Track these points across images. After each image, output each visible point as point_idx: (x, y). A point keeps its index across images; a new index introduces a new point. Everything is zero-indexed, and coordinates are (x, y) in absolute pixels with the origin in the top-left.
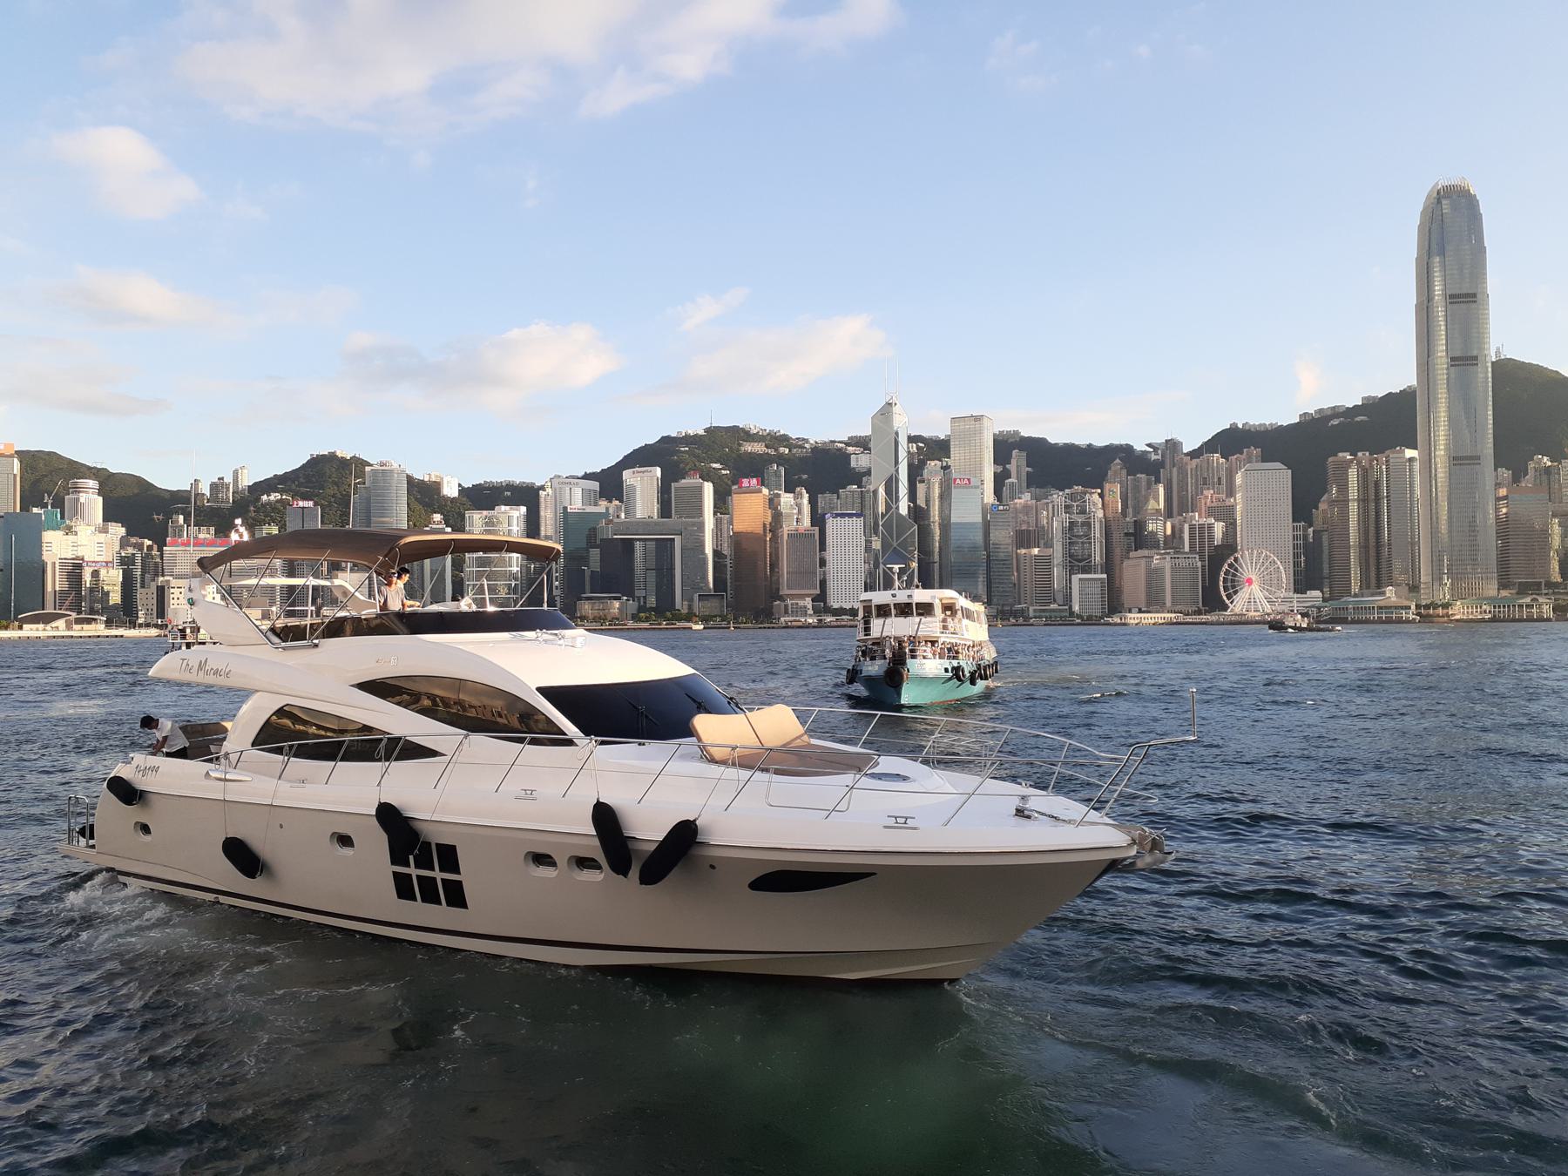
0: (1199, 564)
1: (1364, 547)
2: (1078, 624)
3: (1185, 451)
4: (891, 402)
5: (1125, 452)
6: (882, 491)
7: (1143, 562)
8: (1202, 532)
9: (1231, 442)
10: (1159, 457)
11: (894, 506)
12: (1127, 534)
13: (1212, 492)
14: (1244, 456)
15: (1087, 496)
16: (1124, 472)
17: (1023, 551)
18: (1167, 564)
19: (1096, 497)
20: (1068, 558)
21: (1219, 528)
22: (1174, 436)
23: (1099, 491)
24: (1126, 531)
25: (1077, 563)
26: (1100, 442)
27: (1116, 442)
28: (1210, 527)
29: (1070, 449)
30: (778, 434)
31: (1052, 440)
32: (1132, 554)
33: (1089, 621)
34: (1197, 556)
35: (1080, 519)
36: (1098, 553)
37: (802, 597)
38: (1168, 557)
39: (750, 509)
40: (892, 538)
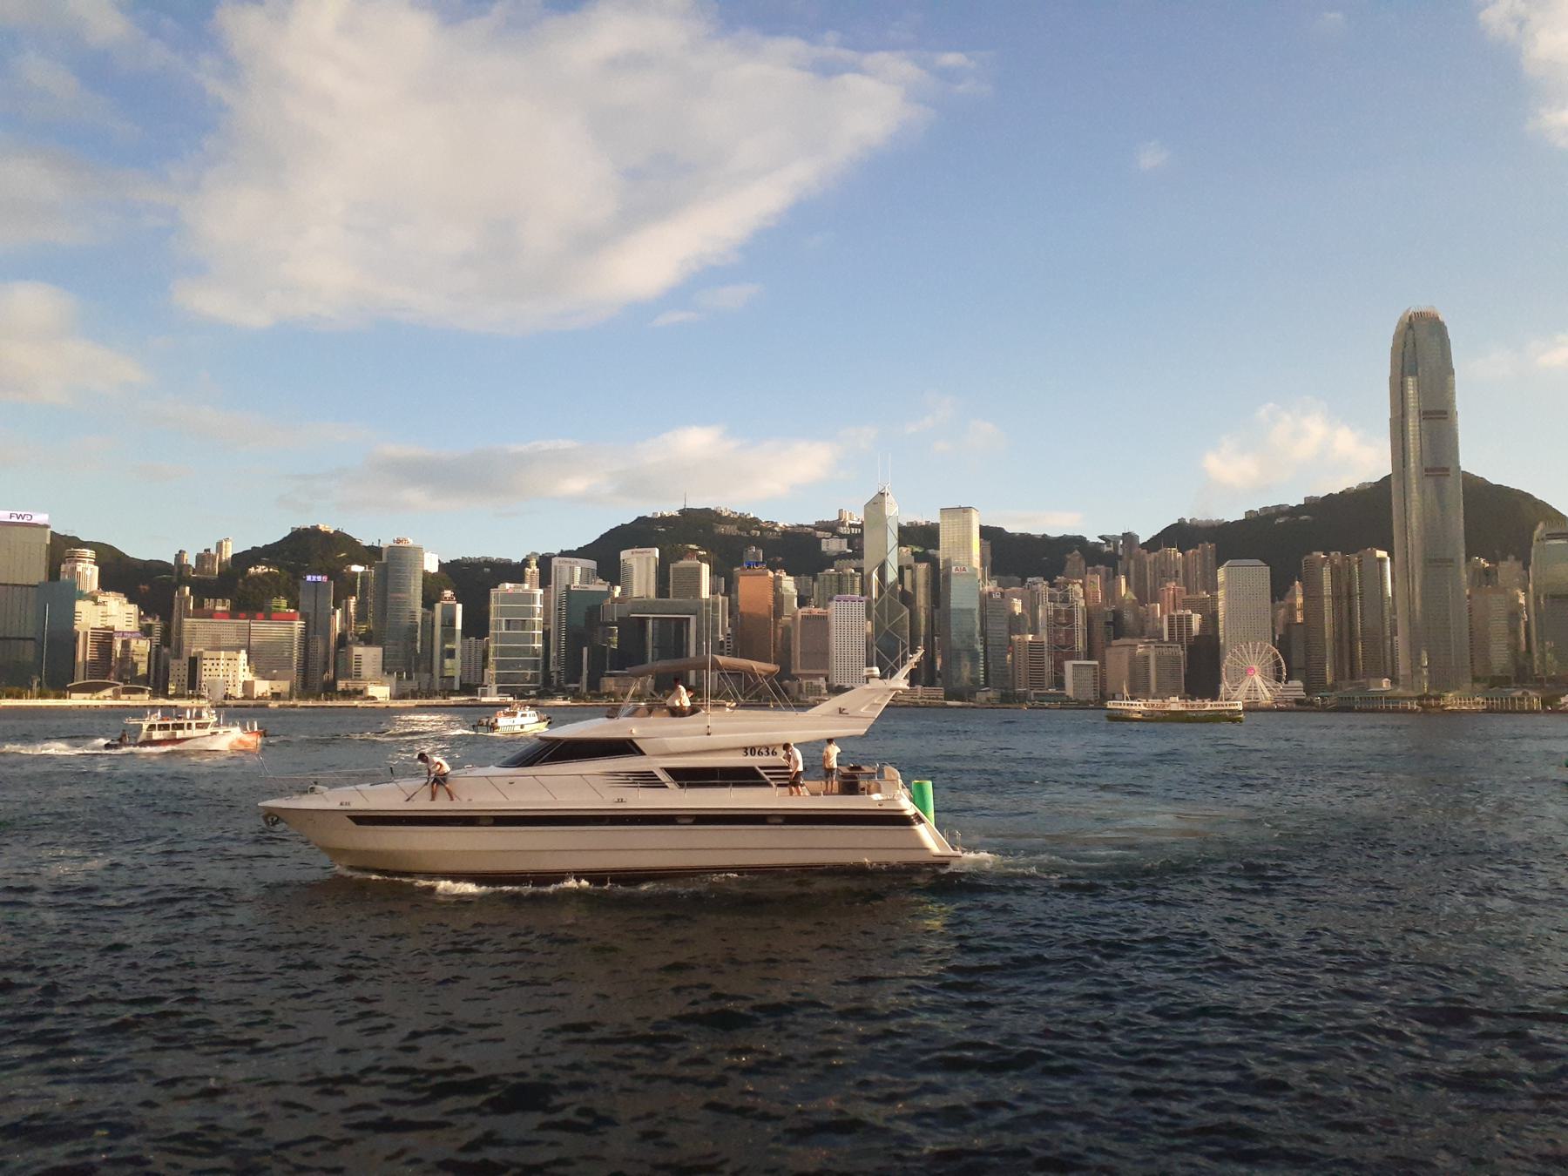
1: (1338, 639)
2: (1092, 709)
3: (1141, 542)
5: (1079, 541)
6: (875, 576)
7: (1127, 649)
8: (1177, 625)
9: (1180, 535)
10: (1111, 549)
12: (1108, 623)
13: (1174, 584)
14: (1198, 551)
15: (1070, 587)
16: (1083, 564)
17: (1017, 637)
19: (1077, 587)
21: (1196, 620)
22: (1131, 530)
23: (1081, 581)
26: (1054, 533)
27: (1069, 533)
28: (1189, 618)
29: (1026, 539)
30: (748, 517)
31: (1010, 529)
32: (1114, 642)
33: (1082, 705)
34: (1180, 646)
35: (1063, 607)
36: (1080, 640)
37: (817, 676)
38: (1152, 646)
39: (755, 587)
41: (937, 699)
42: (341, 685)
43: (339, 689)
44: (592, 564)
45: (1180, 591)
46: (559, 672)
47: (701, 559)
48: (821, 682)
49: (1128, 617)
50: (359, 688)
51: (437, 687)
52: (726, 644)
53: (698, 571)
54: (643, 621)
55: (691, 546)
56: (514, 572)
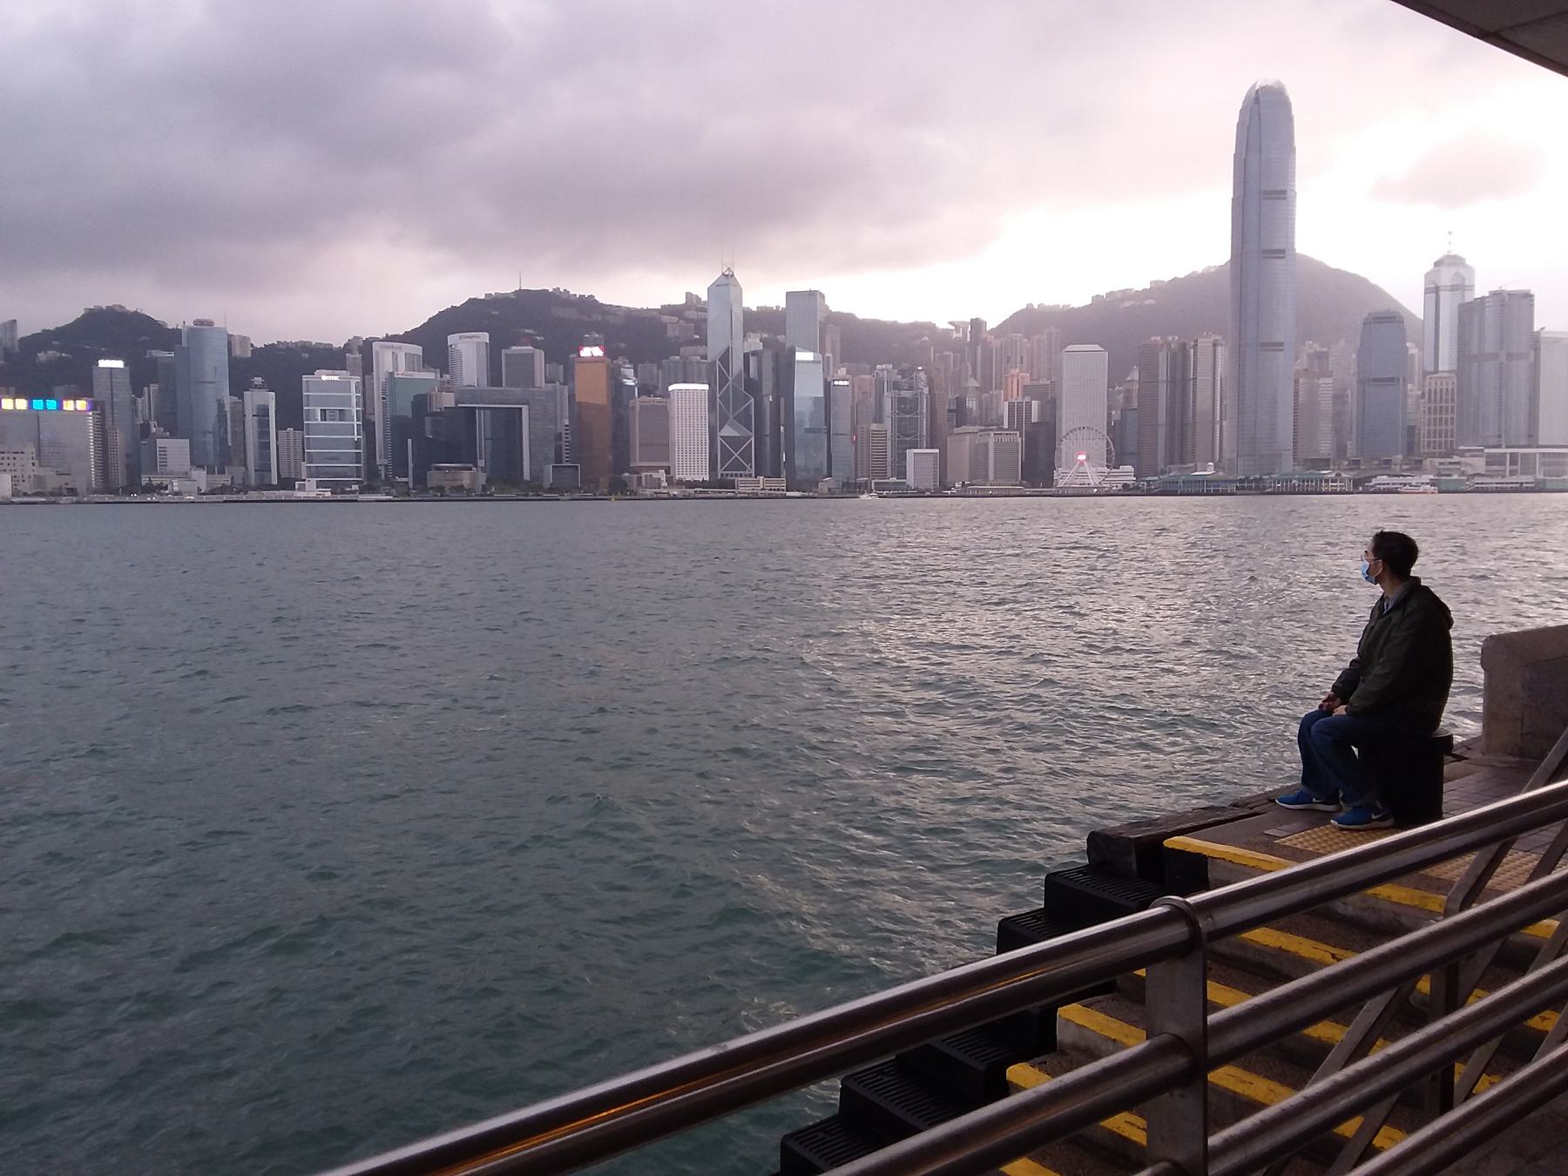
0: (1020, 440)
1: (1171, 425)
4: (727, 273)
11: (730, 379)
12: (949, 411)
18: (991, 442)
20: (897, 434)
21: (1035, 404)
24: (947, 408)
25: (906, 438)
28: (1029, 405)
32: (956, 430)
38: (992, 433)
40: (728, 409)
41: (778, 490)
42: (144, 481)
43: (143, 483)
44: (417, 350)
45: (1022, 377)
46: (386, 466)
47: (537, 345)
48: (662, 474)
49: (971, 404)
50: (165, 484)
51: (253, 483)
52: (564, 436)
53: (530, 357)
54: (471, 412)
55: (527, 331)
56: (330, 358)
